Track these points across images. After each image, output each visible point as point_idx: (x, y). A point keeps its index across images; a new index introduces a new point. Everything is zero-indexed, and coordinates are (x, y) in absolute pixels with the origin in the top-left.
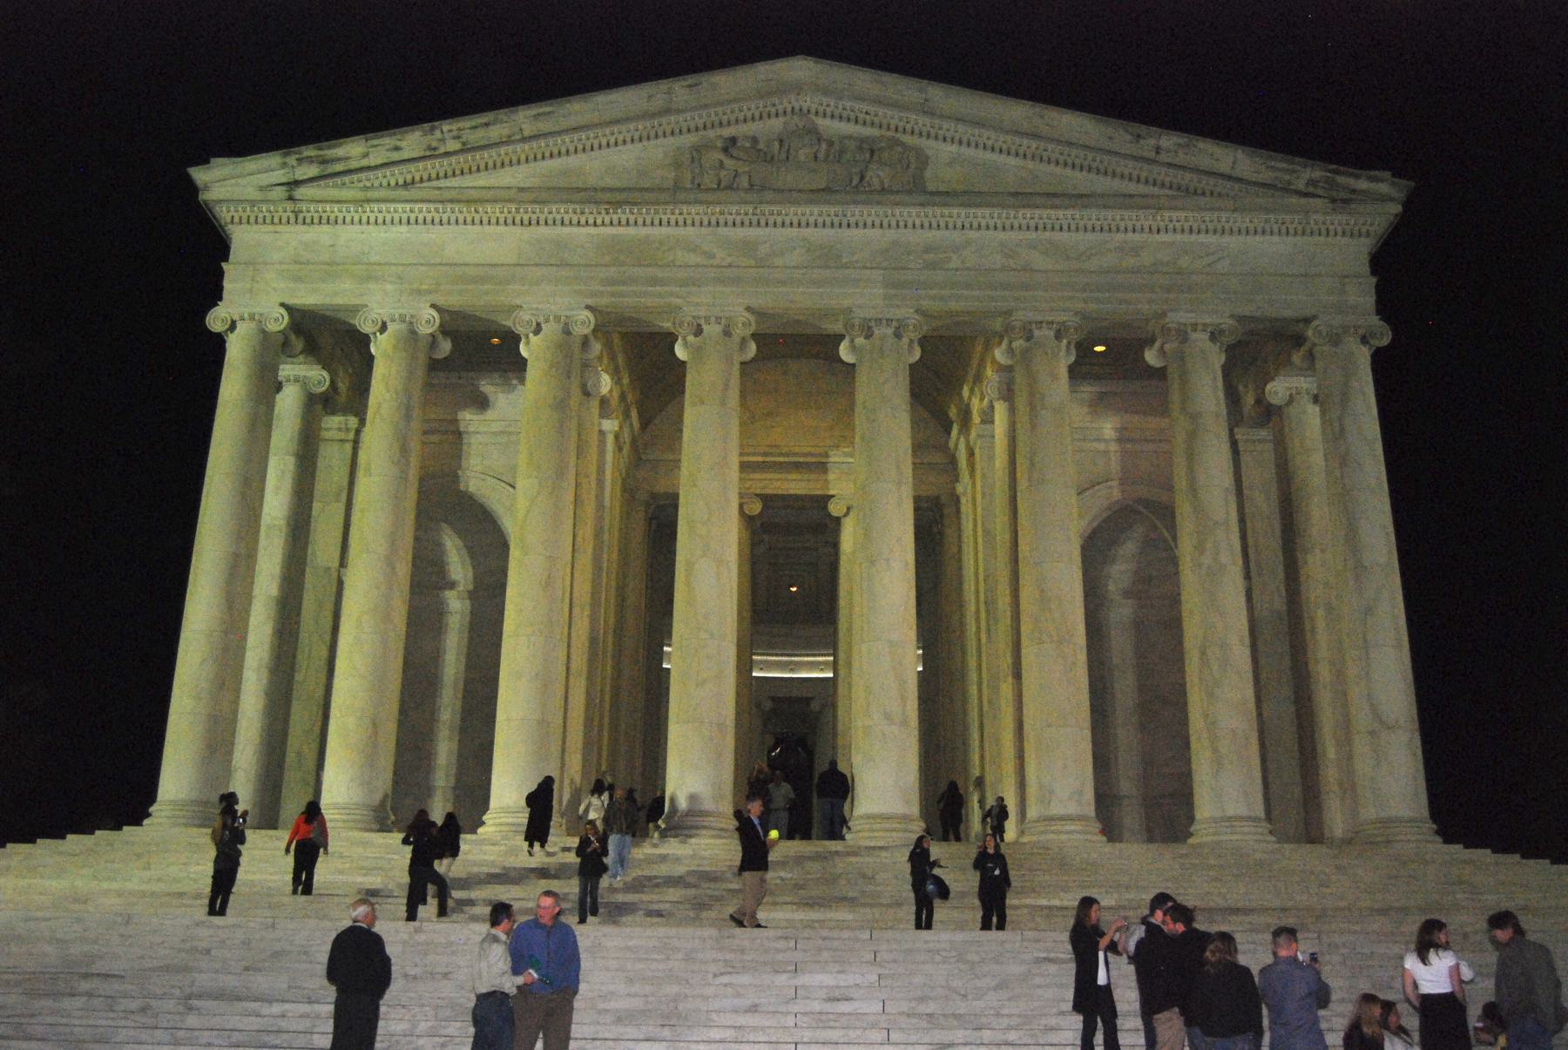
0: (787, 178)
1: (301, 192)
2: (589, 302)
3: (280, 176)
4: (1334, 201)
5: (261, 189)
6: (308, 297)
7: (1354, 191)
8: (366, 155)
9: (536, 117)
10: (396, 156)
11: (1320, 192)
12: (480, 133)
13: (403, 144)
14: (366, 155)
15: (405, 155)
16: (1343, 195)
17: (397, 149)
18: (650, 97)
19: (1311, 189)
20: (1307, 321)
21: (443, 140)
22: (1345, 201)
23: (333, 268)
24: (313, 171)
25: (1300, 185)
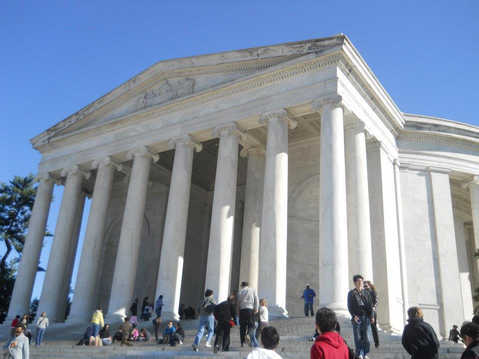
0: (158, 99)
1: (52, 140)
2: (110, 154)
3: (47, 137)
4: (317, 53)
6: (52, 169)
7: (324, 46)
8: (64, 126)
9: (99, 103)
11: (312, 51)
12: (88, 111)
13: (71, 120)
16: (320, 49)
17: (71, 122)
18: (124, 88)
19: (309, 51)
22: (321, 51)
24: (53, 134)
25: (305, 51)
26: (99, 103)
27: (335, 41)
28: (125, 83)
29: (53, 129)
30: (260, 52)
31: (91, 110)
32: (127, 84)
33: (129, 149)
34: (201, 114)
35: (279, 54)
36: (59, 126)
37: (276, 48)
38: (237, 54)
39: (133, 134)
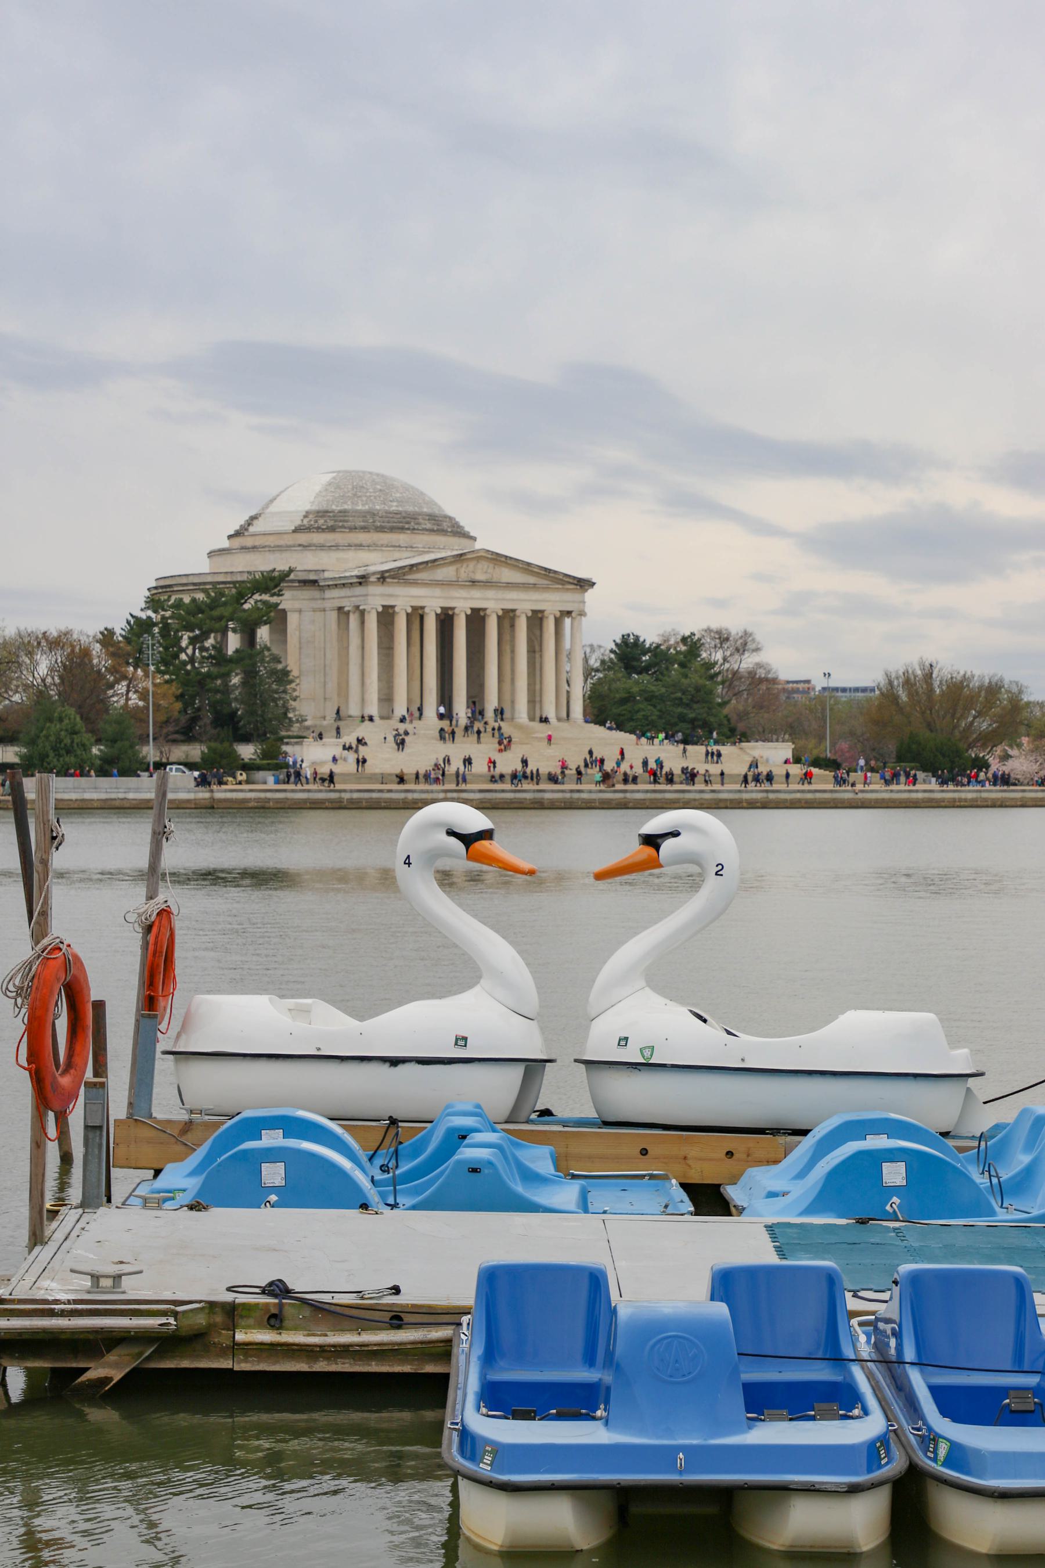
24: (387, 574)
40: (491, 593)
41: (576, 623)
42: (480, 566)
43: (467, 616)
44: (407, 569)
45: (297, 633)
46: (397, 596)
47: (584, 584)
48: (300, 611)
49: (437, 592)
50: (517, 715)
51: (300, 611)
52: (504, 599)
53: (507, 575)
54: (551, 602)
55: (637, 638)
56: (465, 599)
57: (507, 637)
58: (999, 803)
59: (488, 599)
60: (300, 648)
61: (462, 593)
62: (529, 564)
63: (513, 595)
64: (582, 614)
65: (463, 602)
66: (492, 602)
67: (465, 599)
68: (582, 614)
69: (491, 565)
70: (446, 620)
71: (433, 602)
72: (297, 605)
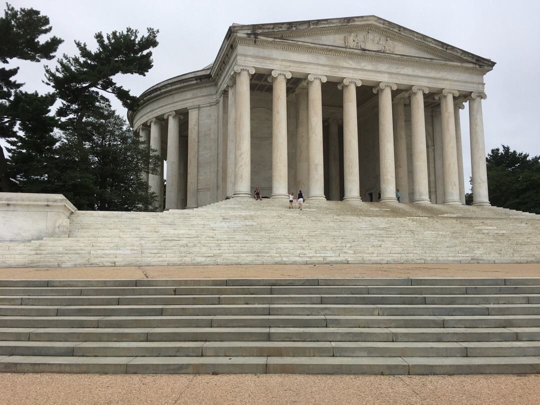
2: (325, 74)
5: (248, 34)
8: (273, 28)
10: (281, 30)
14: (273, 28)
15: (283, 29)
16: (481, 64)
19: (475, 62)
20: (472, 92)
21: (292, 27)
23: (264, 58)
24: (260, 31)
25: (474, 61)
26: (313, 24)
27: (490, 63)
28: (341, 18)
29: (261, 26)
30: (449, 48)
31: (305, 27)
32: (343, 20)
33: (345, 77)
34: (402, 72)
35: (459, 55)
36: (268, 26)
37: (459, 51)
38: (433, 42)
39: (345, 65)
40: (383, 67)
41: (476, 105)
42: (371, 36)
43: (357, 88)
44: (284, 28)
45: (196, 128)
46: (274, 59)
47: (483, 65)
48: (199, 108)
49: (323, 59)
50: (417, 197)
51: (199, 108)
52: (398, 74)
53: (400, 48)
54: (450, 81)
55: (507, 149)
56: (355, 69)
57: (403, 134)
58: (515, 262)
59: (380, 72)
60: (198, 142)
61: (352, 64)
62: (424, 37)
63: (408, 70)
64: (482, 96)
65: (354, 74)
66: (386, 76)
67: (355, 69)
68: (482, 96)
69: (383, 38)
70: (333, 92)
71: (318, 69)
72: (196, 102)
